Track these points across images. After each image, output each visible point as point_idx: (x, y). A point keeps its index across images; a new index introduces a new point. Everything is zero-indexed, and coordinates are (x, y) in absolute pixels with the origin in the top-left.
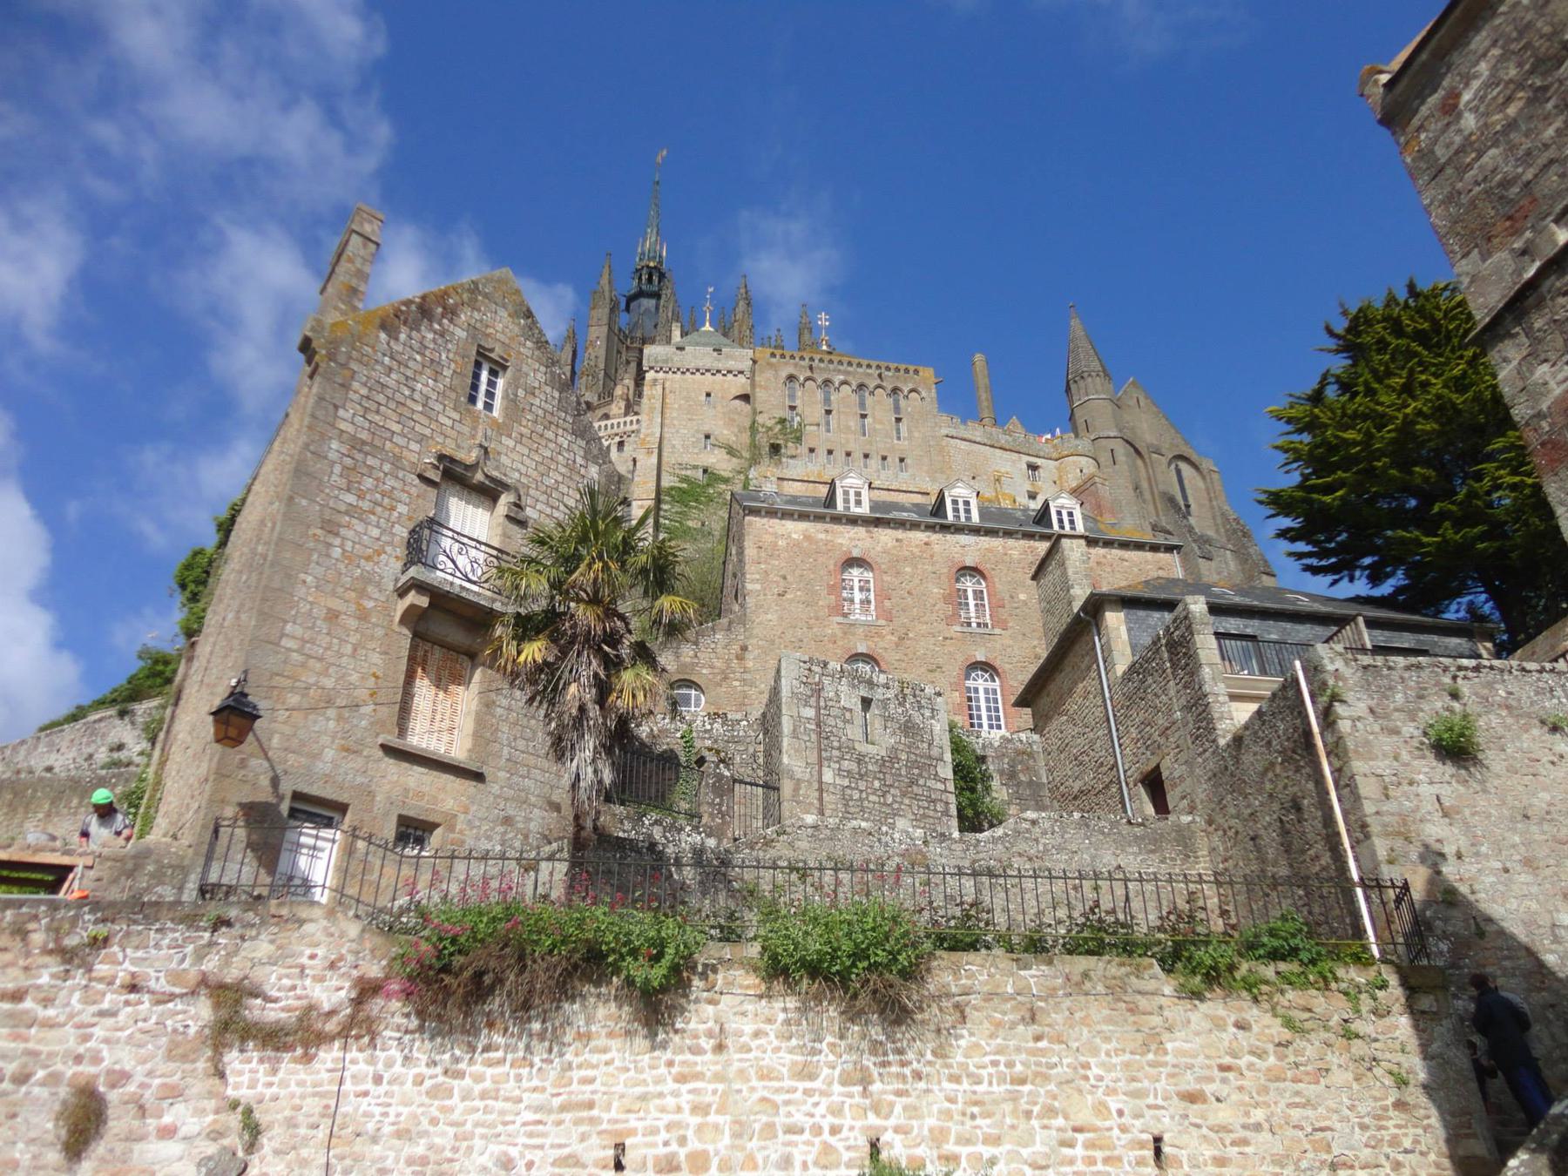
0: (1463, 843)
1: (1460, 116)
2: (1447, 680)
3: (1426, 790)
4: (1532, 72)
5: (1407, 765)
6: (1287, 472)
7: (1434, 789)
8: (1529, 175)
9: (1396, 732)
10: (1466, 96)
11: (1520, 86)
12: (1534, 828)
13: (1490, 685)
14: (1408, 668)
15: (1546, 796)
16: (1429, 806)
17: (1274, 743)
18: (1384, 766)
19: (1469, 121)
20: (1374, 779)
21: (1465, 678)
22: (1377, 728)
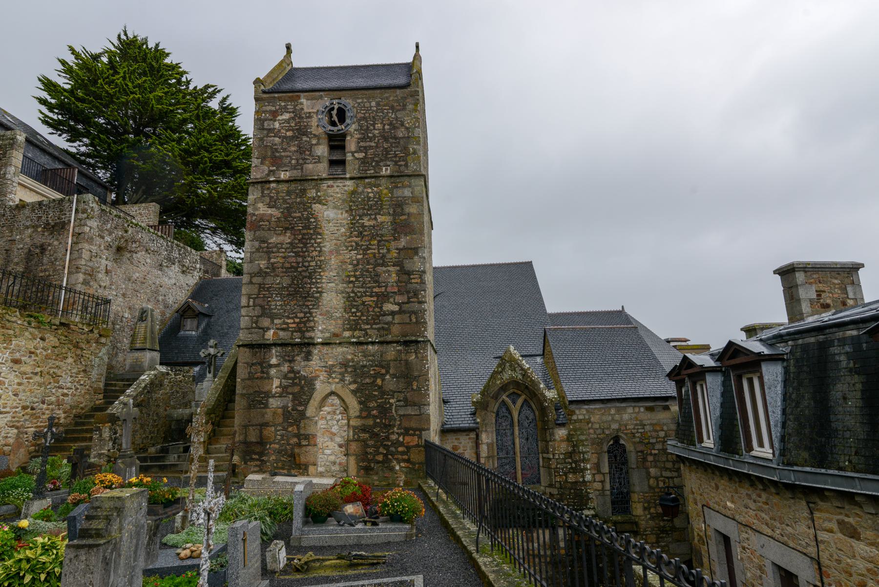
0: (108, 283)
1: (275, 121)
2: (126, 225)
3: (104, 262)
4: (297, 129)
5: (102, 251)
6: (59, 75)
7: (106, 262)
8: (283, 154)
9: (103, 238)
10: (280, 118)
11: (293, 130)
12: (130, 284)
13: (137, 232)
14: (116, 216)
15: (137, 275)
16: (103, 267)
17: (43, 218)
18: (94, 248)
19: (277, 125)
20: (89, 252)
21: (132, 227)
22: (97, 234)
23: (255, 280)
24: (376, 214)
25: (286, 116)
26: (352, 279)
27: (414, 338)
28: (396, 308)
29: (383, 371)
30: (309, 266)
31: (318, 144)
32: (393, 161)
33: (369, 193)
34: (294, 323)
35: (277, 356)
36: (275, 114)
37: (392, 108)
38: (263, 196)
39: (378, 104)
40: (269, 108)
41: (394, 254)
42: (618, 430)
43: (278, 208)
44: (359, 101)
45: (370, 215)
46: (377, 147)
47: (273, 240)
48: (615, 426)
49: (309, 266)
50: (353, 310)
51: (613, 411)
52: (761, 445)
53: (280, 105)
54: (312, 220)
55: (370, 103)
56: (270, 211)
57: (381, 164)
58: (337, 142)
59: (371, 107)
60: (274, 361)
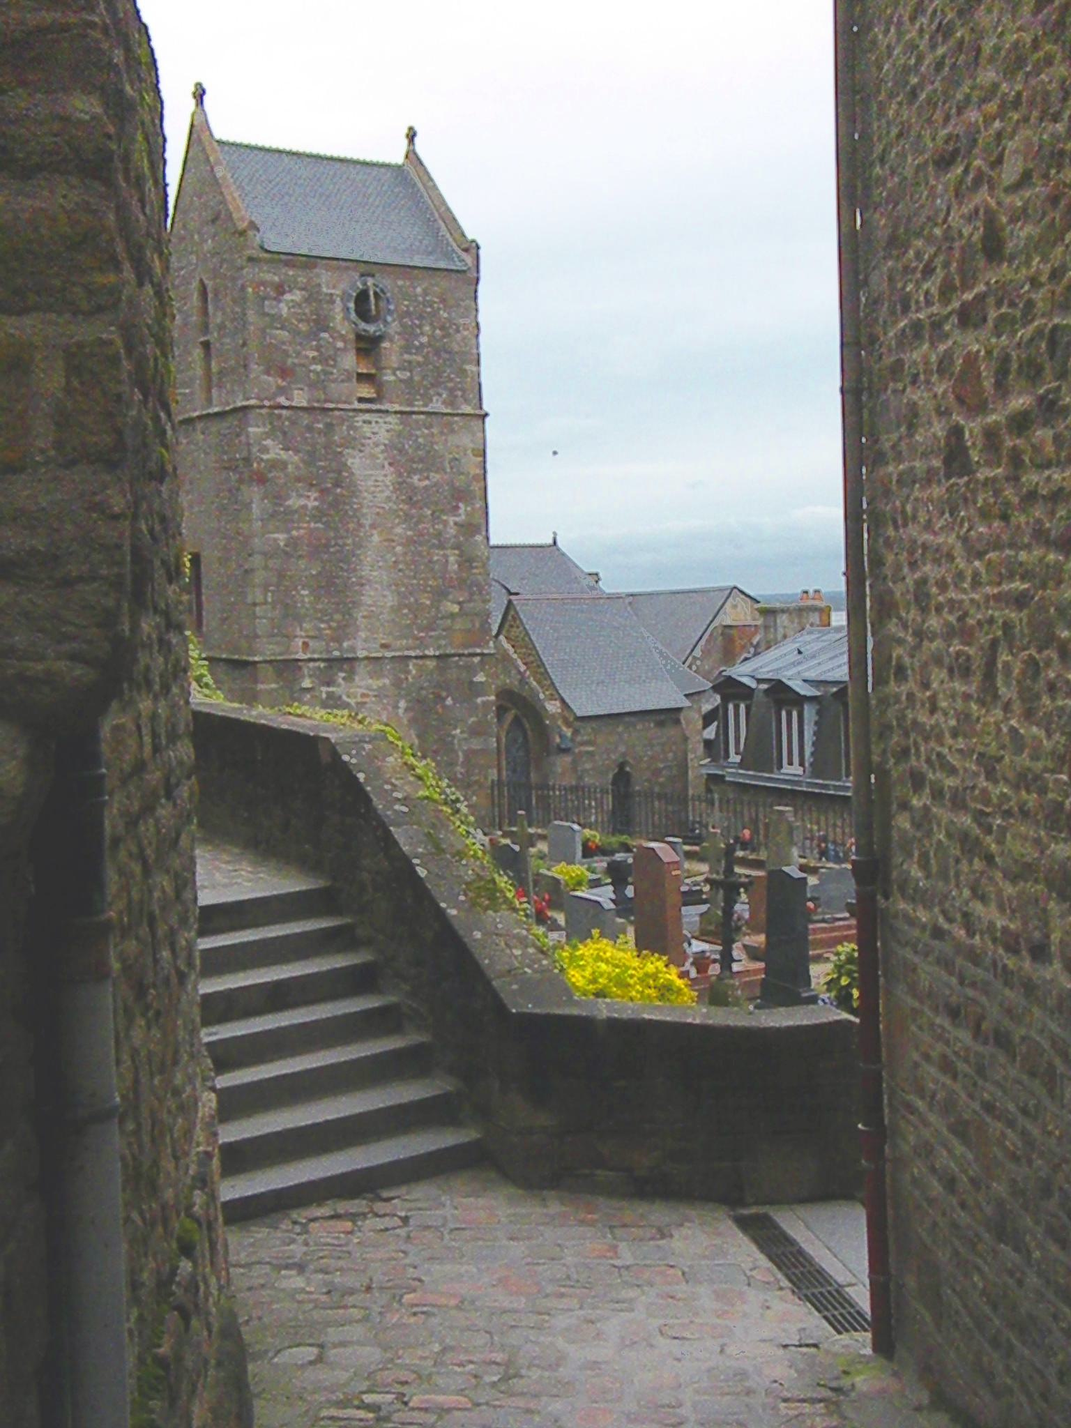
8: (296, 361)
11: (308, 321)
23: (271, 563)
24: (428, 470)
25: (297, 296)
26: (401, 566)
27: (478, 651)
28: (456, 608)
29: (444, 694)
30: (345, 545)
31: (344, 350)
32: (446, 388)
33: (417, 437)
34: (330, 628)
35: (310, 676)
36: (280, 290)
37: (443, 301)
38: (273, 428)
39: (425, 293)
40: (268, 277)
41: (452, 531)
42: (624, 755)
43: (297, 451)
44: (400, 283)
45: (420, 471)
46: (427, 361)
47: (294, 502)
48: (622, 749)
49: (345, 545)
50: (405, 611)
51: (620, 729)
52: (790, 763)
53: (286, 274)
54: (345, 474)
55: (415, 288)
56: (284, 455)
57: (432, 392)
58: (368, 346)
59: (416, 296)
60: (307, 683)
